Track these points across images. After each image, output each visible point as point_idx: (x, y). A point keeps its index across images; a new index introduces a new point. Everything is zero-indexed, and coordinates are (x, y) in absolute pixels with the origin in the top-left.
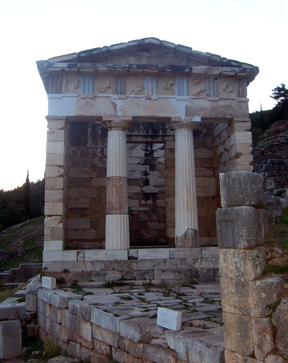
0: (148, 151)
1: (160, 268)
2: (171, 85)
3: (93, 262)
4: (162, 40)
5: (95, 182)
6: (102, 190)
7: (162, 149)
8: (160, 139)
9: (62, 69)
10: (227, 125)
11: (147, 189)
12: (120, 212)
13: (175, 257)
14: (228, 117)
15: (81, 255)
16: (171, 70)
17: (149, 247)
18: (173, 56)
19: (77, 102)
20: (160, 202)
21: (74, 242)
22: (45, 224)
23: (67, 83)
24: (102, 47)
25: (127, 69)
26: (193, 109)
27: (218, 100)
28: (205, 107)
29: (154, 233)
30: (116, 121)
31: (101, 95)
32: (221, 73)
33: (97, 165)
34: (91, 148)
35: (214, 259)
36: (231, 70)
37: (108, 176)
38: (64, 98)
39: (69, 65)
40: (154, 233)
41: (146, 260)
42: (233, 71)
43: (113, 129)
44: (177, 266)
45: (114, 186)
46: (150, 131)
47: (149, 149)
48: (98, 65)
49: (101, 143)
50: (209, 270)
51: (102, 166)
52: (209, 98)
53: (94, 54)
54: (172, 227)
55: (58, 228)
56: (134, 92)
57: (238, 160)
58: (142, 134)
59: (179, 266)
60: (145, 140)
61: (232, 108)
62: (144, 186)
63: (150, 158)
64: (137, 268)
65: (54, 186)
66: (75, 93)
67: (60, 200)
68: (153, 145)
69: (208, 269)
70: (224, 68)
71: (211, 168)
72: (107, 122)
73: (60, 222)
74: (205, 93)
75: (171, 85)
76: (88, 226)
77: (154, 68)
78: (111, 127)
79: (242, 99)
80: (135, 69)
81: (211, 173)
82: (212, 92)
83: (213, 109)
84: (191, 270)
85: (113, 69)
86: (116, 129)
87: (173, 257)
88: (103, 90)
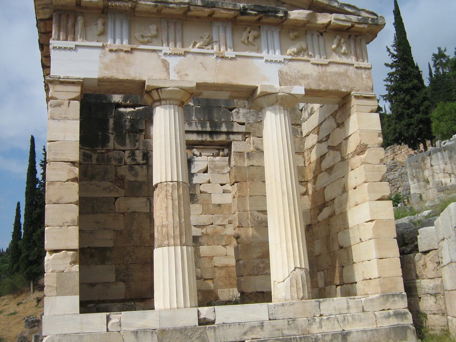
1: (254, 336)
2: (255, 38)
3: (137, 332)
5: (123, 204)
7: (206, 171)
10: (337, 107)
12: (181, 242)
13: (277, 316)
14: (343, 90)
16: (256, 13)
19: (102, 55)
21: (89, 306)
22: (47, 265)
23: (85, 25)
26: (290, 76)
27: (326, 65)
28: (309, 73)
30: (171, 88)
31: (142, 47)
32: (330, 22)
33: (125, 177)
34: (114, 150)
35: (340, 317)
38: (80, 50)
41: (230, 325)
42: (348, 20)
43: (163, 102)
44: (282, 332)
45: (169, 197)
46: (208, 125)
49: (130, 142)
51: (132, 179)
52: (313, 60)
54: (247, 275)
55: (70, 272)
56: (198, 45)
57: (363, 156)
59: (286, 332)
60: (200, 139)
61: (348, 77)
65: (61, 199)
66: (98, 42)
67: (73, 221)
69: (333, 335)
70: (334, 15)
72: (153, 92)
73: (74, 263)
74: (306, 53)
75: (255, 38)
76: (111, 277)
77: (230, 8)
78: (160, 100)
80: (200, 6)
82: (316, 51)
83: (321, 78)
84: (307, 337)
86: (168, 102)
87: (274, 316)
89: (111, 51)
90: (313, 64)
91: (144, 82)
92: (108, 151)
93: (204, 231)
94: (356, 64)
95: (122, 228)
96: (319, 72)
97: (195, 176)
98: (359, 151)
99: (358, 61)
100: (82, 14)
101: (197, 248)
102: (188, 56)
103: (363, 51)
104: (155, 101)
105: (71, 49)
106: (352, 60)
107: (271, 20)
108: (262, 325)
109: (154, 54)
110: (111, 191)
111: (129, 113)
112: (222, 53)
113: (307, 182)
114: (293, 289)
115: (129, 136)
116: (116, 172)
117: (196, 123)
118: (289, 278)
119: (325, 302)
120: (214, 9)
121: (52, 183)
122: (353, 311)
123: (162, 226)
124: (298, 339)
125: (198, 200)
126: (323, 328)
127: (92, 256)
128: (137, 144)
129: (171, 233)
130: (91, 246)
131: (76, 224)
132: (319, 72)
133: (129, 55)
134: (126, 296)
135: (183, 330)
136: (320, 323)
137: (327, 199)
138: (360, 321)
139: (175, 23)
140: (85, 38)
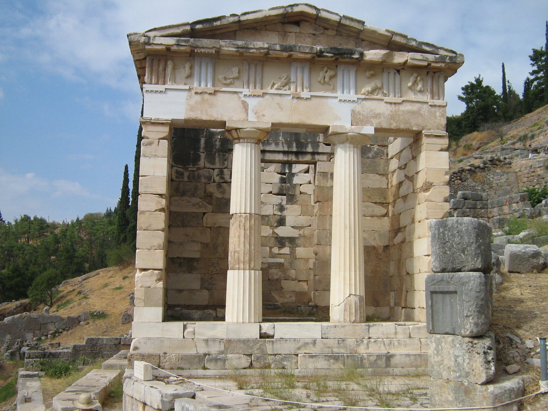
0: (284, 174)
2: (331, 78)
3: (207, 340)
4: (320, 8)
6: (222, 233)
8: (308, 158)
9: (166, 48)
10: (412, 140)
11: (282, 232)
13: (329, 336)
14: (414, 129)
15: (190, 329)
16: (332, 55)
17: (287, 318)
18: (335, 33)
19: (188, 98)
20: (300, 251)
21: (177, 309)
22: (137, 281)
23: (174, 69)
24: (229, 16)
25: (266, 51)
26: (362, 115)
27: (399, 104)
29: (291, 297)
32: (407, 60)
35: (387, 341)
36: (421, 58)
37: (232, 211)
38: (169, 92)
39: (178, 41)
40: (291, 297)
43: (241, 140)
46: (294, 145)
47: (287, 171)
48: (222, 43)
49: (219, 161)
50: (379, 357)
51: (220, 196)
52: (386, 99)
53: (217, 26)
55: (155, 288)
56: (276, 86)
57: (427, 194)
58: (282, 150)
59: (335, 350)
60: (286, 159)
61: (421, 115)
62: (277, 226)
63: (288, 184)
64: (273, 351)
65: (149, 226)
66: (185, 84)
67: (159, 246)
68: (294, 165)
69: (377, 356)
71: (383, 203)
73: (159, 280)
74: (380, 92)
75: (331, 78)
76: (197, 285)
77: (307, 51)
78: (239, 138)
79: (437, 102)
81: (383, 211)
82: (391, 90)
83: (392, 117)
85: (244, 50)
86: (246, 140)
88: (228, 81)
89: (196, 93)
90: (386, 103)
91: (225, 122)
92: (199, 169)
93: (301, 232)
94: (431, 102)
95: (209, 241)
96: (391, 111)
97: (296, 176)
98: (425, 188)
99: (433, 99)
100: (172, 59)
101: (293, 250)
102: (267, 97)
103: (440, 88)
104: (235, 139)
105: (161, 92)
106: (426, 97)
107: (347, 60)
108: (314, 342)
109: (235, 96)
110: (200, 207)
111: (220, 132)
112: (298, 94)
113: (388, 203)
114: (346, 313)
115: (219, 155)
116: (205, 188)
117: (283, 143)
118: (343, 304)
119: (375, 327)
120: (292, 53)
121: (143, 212)
122: (400, 336)
123: (235, 252)
124: (346, 357)
125: (297, 201)
126: (370, 349)
127: (180, 265)
128: (226, 163)
129: (242, 258)
130: (180, 256)
131: (162, 248)
132: (391, 111)
133: (212, 97)
134: (209, 303)
135: (245, 342)
136: (368, 344)
137: (401, 226)
138: (405, 346)
139: (256, 64)
140: (174, 81)
